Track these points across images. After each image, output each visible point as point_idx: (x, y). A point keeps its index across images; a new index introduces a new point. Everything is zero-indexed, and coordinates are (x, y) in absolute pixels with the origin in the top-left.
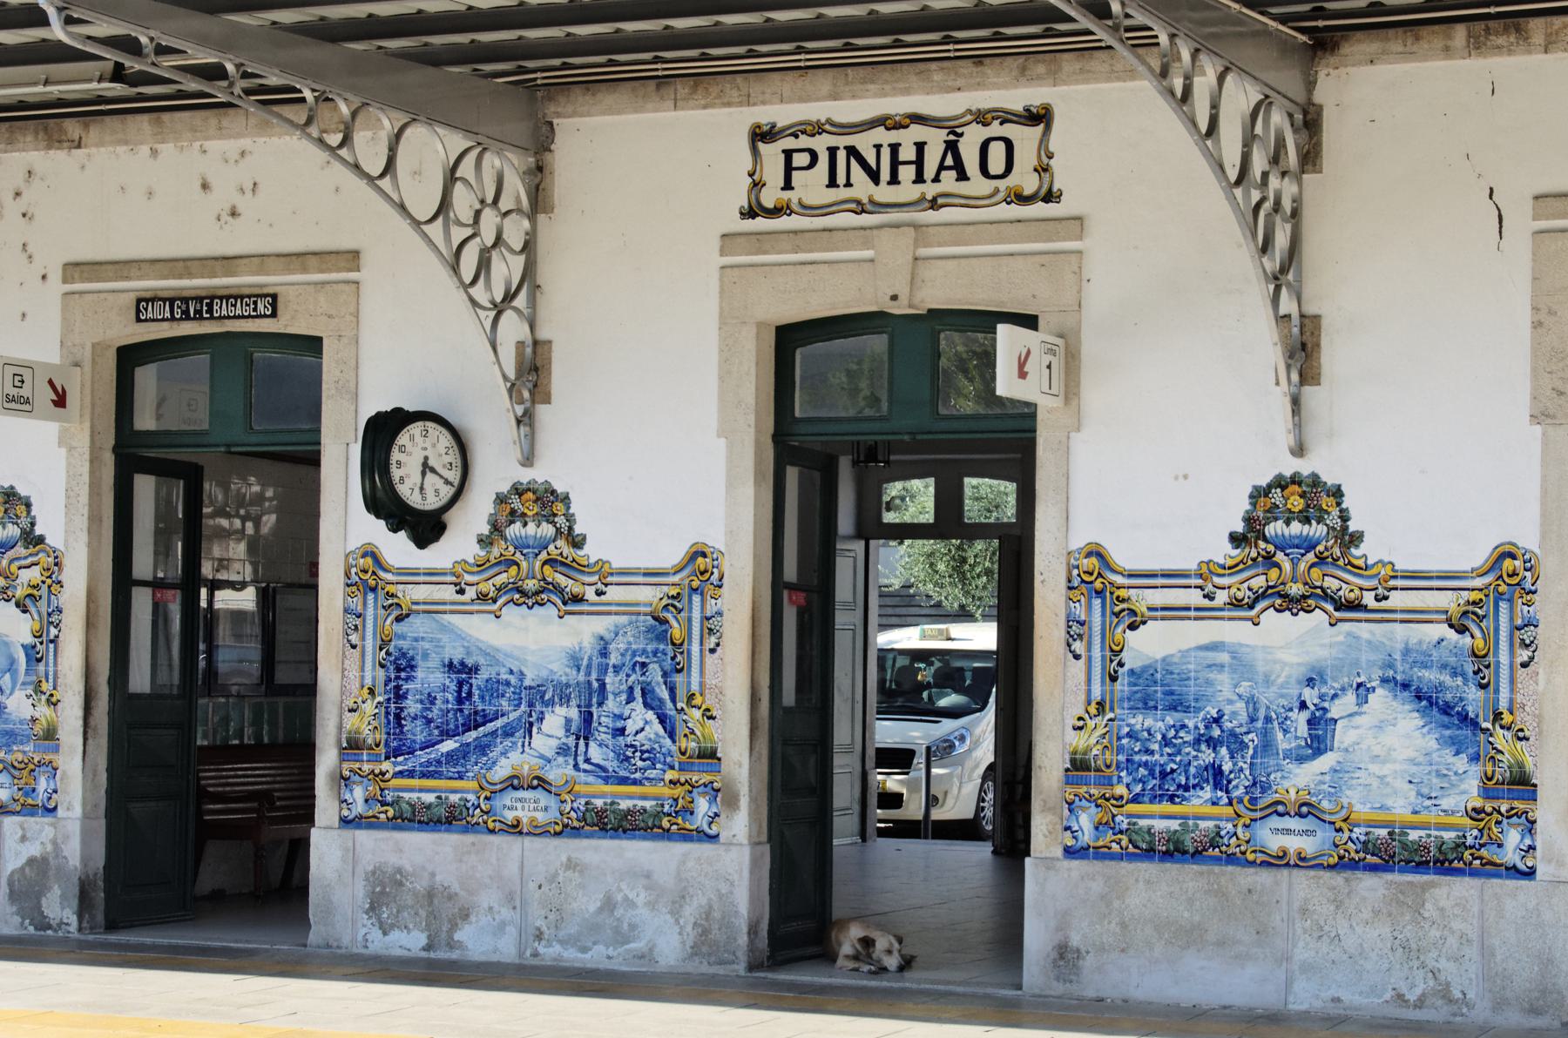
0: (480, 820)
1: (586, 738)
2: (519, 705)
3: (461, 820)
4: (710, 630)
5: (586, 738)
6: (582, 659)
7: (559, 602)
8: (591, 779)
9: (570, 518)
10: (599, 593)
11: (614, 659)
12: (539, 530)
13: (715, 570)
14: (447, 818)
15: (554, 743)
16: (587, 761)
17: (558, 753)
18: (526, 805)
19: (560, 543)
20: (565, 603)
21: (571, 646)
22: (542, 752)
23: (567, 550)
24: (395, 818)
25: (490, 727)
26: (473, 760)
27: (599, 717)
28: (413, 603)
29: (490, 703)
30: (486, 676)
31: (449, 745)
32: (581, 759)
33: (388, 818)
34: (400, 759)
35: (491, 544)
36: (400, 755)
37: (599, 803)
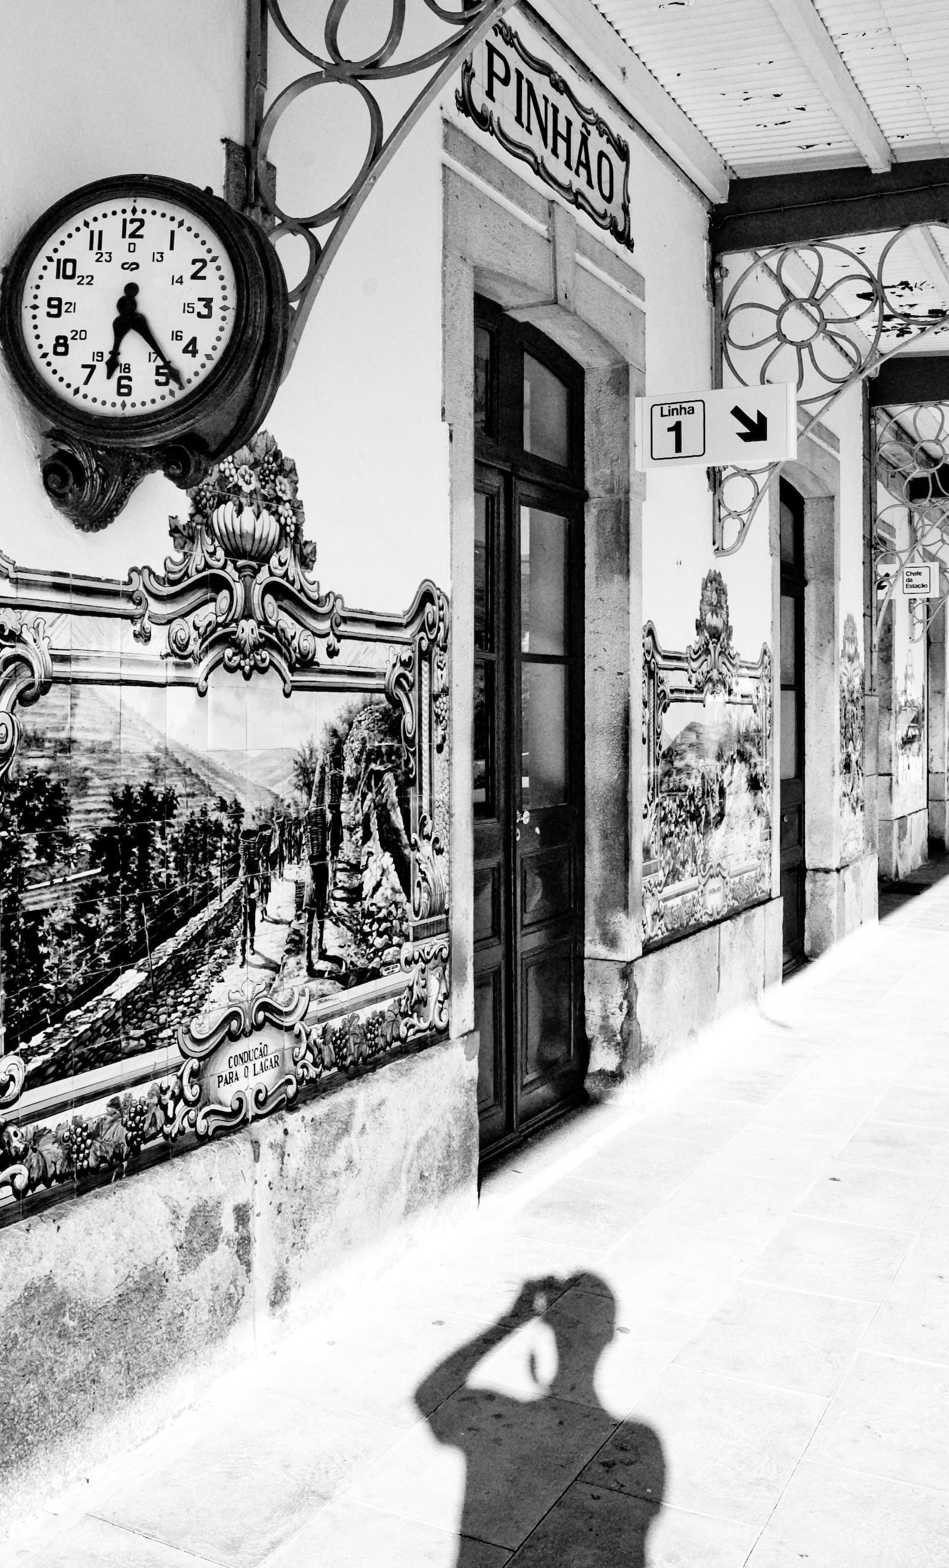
0: (186, 1123)
1: (321, 916)
2: (233, 873)
3: (154, 1137)
4: (438, 716)
5: (321, 916)
6: (313, 772)
7: (284, 666)
8: (327, 985)
9: (297, 508)
10: (332, 653)
11: (349, 770)
12: (259, 523)
13: (441, 624)
14: (129, 1142)
15: (282, 933)
16: (323, 955)
17: (288, 951)
18: (250, 1065)
19: (286, 553)
20: (292, 669)
21: (300, 750)
22: (267, 955)
23: (294, 569)
24: (32, 1184)
25: (195, 924)
26: (170, 1001)
27: (335, 872)
28: (55, 658)
29: (193, 875)
30: (184, 820)
31: (129, 981)
32: (315, 953)
33: (16, 1193)
34: (37, 1039)
35: (192, 539)
36: (36, 1032)
37: (336, 1024)
